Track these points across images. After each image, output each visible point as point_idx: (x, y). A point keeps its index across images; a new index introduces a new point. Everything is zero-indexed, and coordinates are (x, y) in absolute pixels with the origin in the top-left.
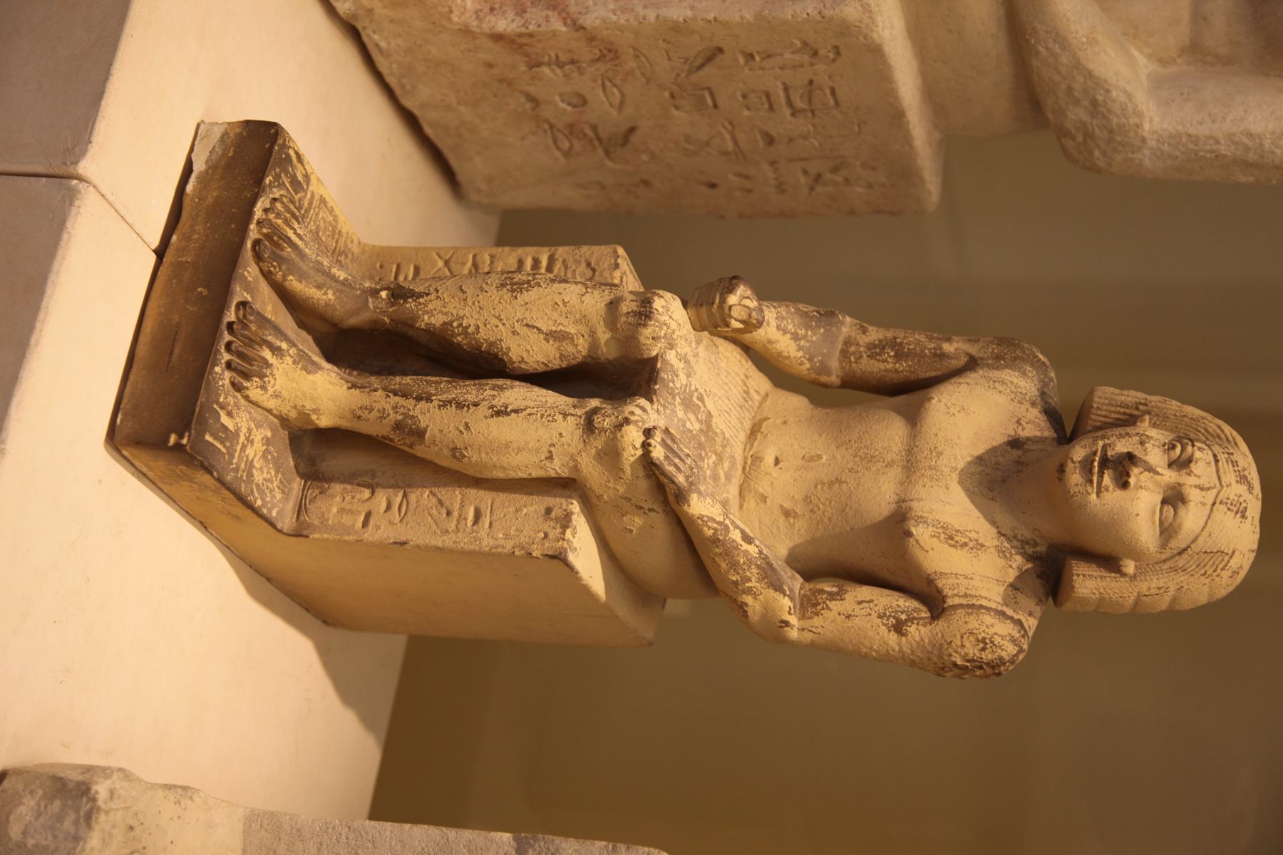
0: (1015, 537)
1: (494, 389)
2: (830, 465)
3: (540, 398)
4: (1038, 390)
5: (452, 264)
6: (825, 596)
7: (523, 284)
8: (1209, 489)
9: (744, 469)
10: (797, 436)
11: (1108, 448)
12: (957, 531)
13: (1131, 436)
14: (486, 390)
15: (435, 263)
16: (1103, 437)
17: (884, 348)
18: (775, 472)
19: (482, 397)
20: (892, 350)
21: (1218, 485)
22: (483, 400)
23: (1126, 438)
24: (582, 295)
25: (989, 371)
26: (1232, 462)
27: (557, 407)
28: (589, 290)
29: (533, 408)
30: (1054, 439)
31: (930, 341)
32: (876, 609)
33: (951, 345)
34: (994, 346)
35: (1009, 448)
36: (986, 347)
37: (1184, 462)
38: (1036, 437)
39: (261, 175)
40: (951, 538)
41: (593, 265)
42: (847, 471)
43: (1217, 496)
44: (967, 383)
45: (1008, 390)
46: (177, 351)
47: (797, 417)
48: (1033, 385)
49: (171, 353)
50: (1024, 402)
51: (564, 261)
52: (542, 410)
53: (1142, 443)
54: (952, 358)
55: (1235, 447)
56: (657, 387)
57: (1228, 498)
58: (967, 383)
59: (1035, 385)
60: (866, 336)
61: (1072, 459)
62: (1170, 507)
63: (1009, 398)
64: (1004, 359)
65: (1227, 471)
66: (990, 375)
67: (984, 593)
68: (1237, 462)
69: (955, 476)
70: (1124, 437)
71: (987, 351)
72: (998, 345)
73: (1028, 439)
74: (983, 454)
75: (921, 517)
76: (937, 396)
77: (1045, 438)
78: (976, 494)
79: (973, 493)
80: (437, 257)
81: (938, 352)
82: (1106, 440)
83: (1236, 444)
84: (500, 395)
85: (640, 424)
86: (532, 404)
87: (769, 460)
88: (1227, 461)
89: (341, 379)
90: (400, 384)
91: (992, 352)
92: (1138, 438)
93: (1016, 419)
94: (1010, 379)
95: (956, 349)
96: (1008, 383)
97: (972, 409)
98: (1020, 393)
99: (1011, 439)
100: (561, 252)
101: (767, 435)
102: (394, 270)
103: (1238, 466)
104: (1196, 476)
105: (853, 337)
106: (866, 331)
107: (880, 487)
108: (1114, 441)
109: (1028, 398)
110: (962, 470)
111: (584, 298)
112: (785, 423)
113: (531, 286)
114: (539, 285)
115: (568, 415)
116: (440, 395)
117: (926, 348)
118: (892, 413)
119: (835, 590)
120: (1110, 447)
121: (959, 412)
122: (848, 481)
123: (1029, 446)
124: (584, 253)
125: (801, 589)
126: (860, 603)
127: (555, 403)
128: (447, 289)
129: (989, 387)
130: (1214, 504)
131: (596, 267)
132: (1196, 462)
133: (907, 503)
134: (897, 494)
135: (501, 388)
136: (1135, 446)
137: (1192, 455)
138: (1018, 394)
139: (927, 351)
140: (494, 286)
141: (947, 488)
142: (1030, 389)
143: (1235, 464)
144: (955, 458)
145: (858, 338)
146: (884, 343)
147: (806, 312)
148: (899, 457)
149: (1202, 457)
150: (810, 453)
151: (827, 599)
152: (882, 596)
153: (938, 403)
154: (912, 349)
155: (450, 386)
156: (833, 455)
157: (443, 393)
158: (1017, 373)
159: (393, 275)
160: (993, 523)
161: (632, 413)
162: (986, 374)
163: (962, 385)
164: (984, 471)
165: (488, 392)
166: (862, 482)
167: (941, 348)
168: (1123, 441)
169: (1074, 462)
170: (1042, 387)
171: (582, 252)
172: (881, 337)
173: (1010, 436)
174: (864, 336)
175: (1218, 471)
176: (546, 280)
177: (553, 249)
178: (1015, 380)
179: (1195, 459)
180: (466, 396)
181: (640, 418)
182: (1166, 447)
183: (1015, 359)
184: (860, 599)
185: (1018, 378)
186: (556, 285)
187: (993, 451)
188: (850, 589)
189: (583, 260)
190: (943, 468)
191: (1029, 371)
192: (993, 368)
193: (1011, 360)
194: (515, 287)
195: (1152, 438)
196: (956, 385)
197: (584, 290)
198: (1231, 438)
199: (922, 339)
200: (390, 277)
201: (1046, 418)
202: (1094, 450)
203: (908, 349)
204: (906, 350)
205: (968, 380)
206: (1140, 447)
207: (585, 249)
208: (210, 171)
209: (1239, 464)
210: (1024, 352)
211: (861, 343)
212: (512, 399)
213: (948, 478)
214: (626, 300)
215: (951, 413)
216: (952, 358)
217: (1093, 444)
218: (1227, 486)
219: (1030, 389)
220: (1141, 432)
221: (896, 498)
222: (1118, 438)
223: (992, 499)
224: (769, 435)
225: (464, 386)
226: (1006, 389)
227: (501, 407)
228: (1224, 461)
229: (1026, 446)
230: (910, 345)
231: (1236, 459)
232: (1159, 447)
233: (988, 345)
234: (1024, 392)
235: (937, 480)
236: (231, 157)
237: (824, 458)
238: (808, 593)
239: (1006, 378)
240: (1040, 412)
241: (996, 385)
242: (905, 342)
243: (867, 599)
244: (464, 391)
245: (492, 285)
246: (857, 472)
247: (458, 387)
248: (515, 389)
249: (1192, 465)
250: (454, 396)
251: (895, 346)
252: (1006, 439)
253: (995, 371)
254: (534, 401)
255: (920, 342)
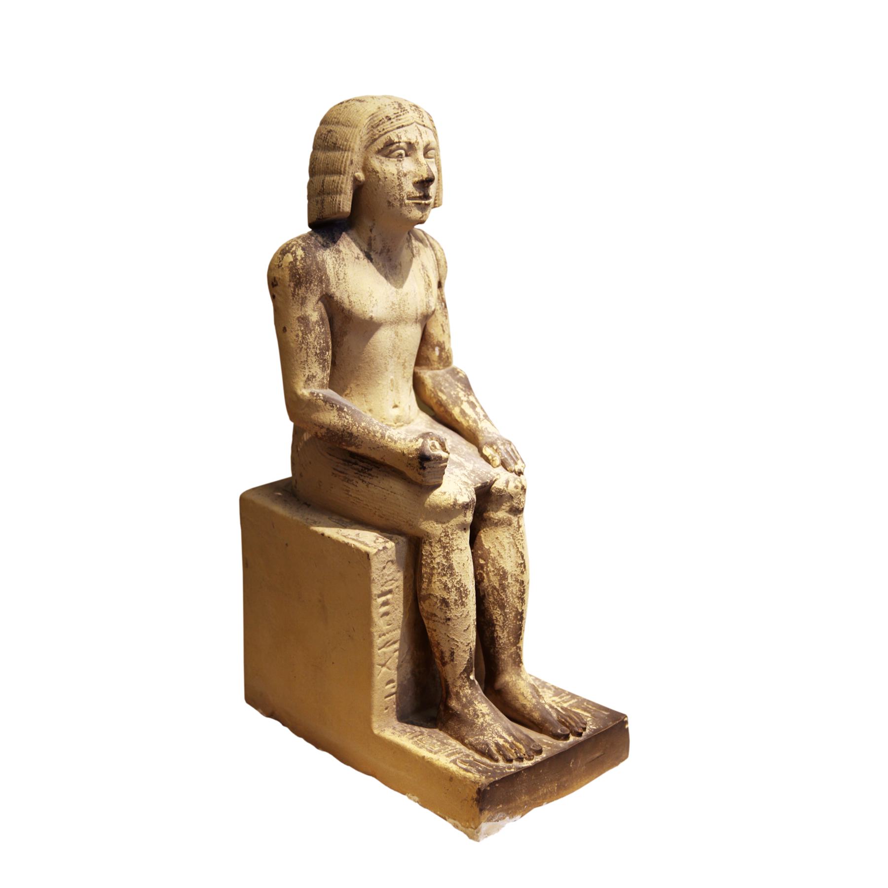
0: (409, 246)
1: (507, 578)
2: (395, 372)
3: (507, 547)
4: (325, 250)
5: (383, 662)
6: (443, 353)
7: (461, 591)
8: (419, 130)
9: (402, 426)
10: (381, 399)
11: (411, 196)
12: (425, 282)
13: (402, 183)
14: (509, 583)
15: (385, 673)
16: (402, 200)
17: (325, 359)
18: (402, 405)
19: (513, 583)
20: (326, 354)
21: (415, 124)
22: (517, 581)
23: (402, 185)
24: (461, 550)
25: (332, 285)
26: (397, 117)
27: (513, 535)
28: (455, 548)
29: (518, 548)
30: (348, 235)
31: (314, 330)
32: (444, 321)
33: (312, 316)
34: (312, 285)
35: (373, 261)
36: (312, 291)
37: (408, 146)
38: (356, 245)
39: (514, 776)
40: (429, 284)
41: (384, 565)
42: (399, 361)
43: (420, 124)
44: (348, 297)
45: (340, 269)
46: (597, 755)
47: (363, 404)
48: (325, 254)
49: (598, 757)
50: (341, 257)
51: (382, 586)
52: (519, 542)
53: (405, 175)
54: (321, 312)
55: (374, 115)
56: (488, 480)
57: (420, 117)
58: (348, 297)
59: (324, 253)
60: (316, 375)
61: (420, 218)
62: (428, 153)
63: (344, 267)
64: (322, 277)
65: (407, 119)
66: (334, 283)
67: (432, 259)
68: (395, 114)
69: (400, 291)
70: (402, 187)
71: (315, 290)
72: (311, 283)
73: (361, 250)
74: (383, 276)
75: (426, 305)
76: (369, 313)
77: (352, 239)
78: (402, 275)
79: (403, 277)
80: (380, 674)
81: (321, 323)
82: (405, 198)
83: (373, 114)
84: (510, 573)
85: (519, 480)
86: (513, 551)
87: (396, 412)
88: (400, 120)
89: (521, 671)
90: (508, 637)
91: (317, 286)
92: (402, 178)
93: (357, 260)
94: (332, 270)
95: (314, 311)
96: (335, 270)
97: (368, 289)
98: (337, 261)
99: (369, 261)
100: (375, 591)
101: (384, 419)
102: (389, 698)
103: (398, 113)
104: (417, 138)
105: (319, 383)
106: (313, 375)
107: (409, 336)
108: (405, 193)
109: (337, 256)
110: (395, 287)
111: (463, 548)
112: (370, 410)
113: (462, 585)
114: (460, 580)
115: (519, 525)
116: (517, 608)
117: (321, 332)
118: (371, 341)
119: (437, 349)
120: (409, 195)
121: (373, 297)
122: (404, 358)
123: (365, 247)
124: (377, 574)
125: (438, 369)
126: (444, 331)
127: (509, 538)
128: (466, 639)
129: (345, 282)
130: (424, 126)
131: (387, 561)
132: (410, 139)
133: (418, 316)
134: (412, 324)
135: (503, 575)
136: (408, 179)
137: (406, 142)
138: (338, 262)
139: (322, 330)
140: (464, 609)
141: (407, 294)
142: (328, 255)
143: (397, 116)
144: (392, 293)
145: (318, 380)
146: (321, 361)
147: (352, 416)
148: (393, 329)
149: (406, 136)
150: (390, 387)
151: (444, 352)
152: (437, 320)
153: (374, 312)
154: (323, 341)
155: (508, 606)
156: (390, 372)
157: (514, 607)
158: (327, 266)
159: (392, 697)
160: (411, 261)
161: (516, 487)
162: (334, 286)
163: (352, 300)
164: (389, 274)
165: (510, 580)
166: (406, 349)
167: (317, 322)
168: (405, 187)
169: (423, 216)
170: (320, 247)
171: (376, 576)
172: (316, 364)
173: (368, 262)
174: (317, 377)
175: (408, 125)
176: (452, 579)
177: (373, 596)
178: (331, 266)
179: (409, 141)
180: (515, 593)
181: (516, 482)
182: (401, 159)
183: (319, 269)
184: (442, 332)
185: (329, 265)
186: (457, 570)
187: (379, 270)
188: (436, 340)
189: (382, 573)
190: (398, 299)
191: (320, 258)
192: (329, 282)
193: (321, 272)
194: (464, 595)
195: (398, 169)
196: (353, 304)
197: (456, 551)
198: (369, 118)
199: (313, 336)
200: (393, 698)
201: (339, 241)
202: (413, 205)
203: (324, 343)
204: (324, 344)
205: (345, 297)
206: (407, 176)
207: (374, 576)
208: (510, 812)
209: (396, 112)
210: (311, 265)
211: (323, 376)
212: (512, 564)
213: (402, 294)
214: (465, 520)
215: (376, 302)
216: (321, 312)
217: (409, 205)
218: (413, 118)
219: (328, 255)
220: (396, 176)
221: (414, 324)
222: (403, 190)
223: (400, 265)
224: (385, 417)
225: (506, 597)
226: (341, 271)
227: (522, 567)
228: (400, 122)
229: (366, 250)
230: (320, 343)
231: (392, 114)
232: (402, 164)
233: (310, 290)
234: (334, 259)
235: (405, 301)
236: (502, 804)
237: (392, 377)
238: (442, 364)
239: (333, 272)
240: (339, 246)
241: (341, 278)
242: (319, 347)
243: (441, 328)
244: (510, 595)
245: (463, 611)
246: (400, 354)
247: (508, 601)
248: (503, 566)
249: (412, 141)
250: (516, 600)
251: (323, 353)
252: (371, 264)
253: (331, 281)
254: (510, 550)
255: (316, 338)
